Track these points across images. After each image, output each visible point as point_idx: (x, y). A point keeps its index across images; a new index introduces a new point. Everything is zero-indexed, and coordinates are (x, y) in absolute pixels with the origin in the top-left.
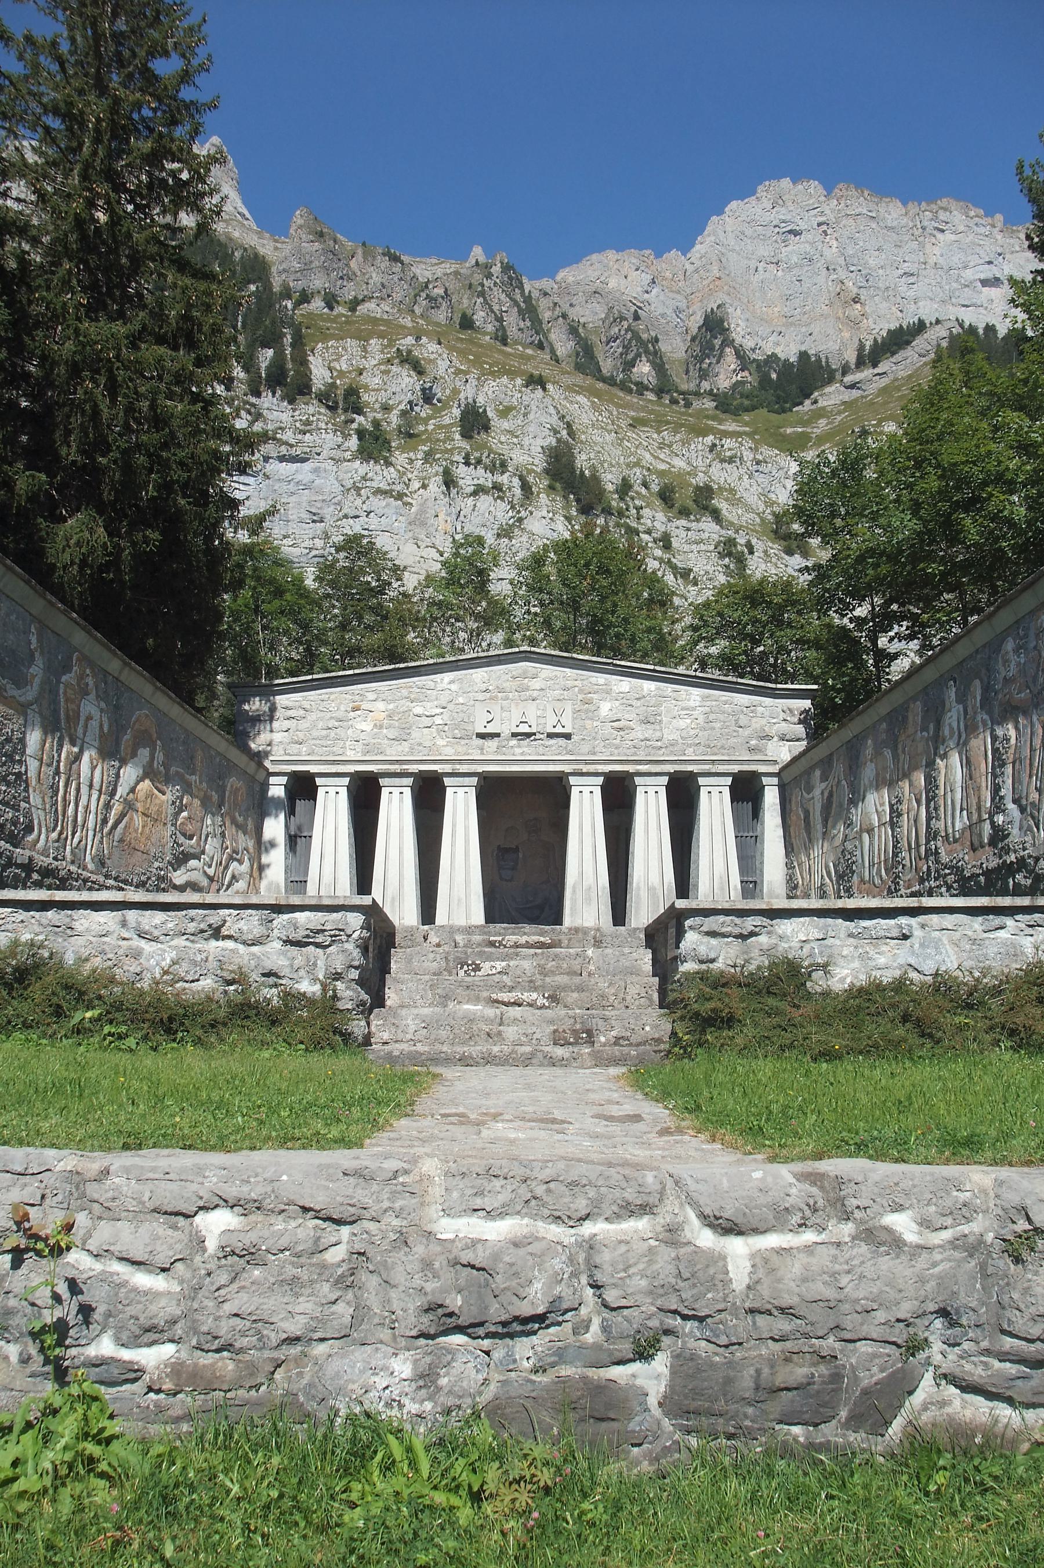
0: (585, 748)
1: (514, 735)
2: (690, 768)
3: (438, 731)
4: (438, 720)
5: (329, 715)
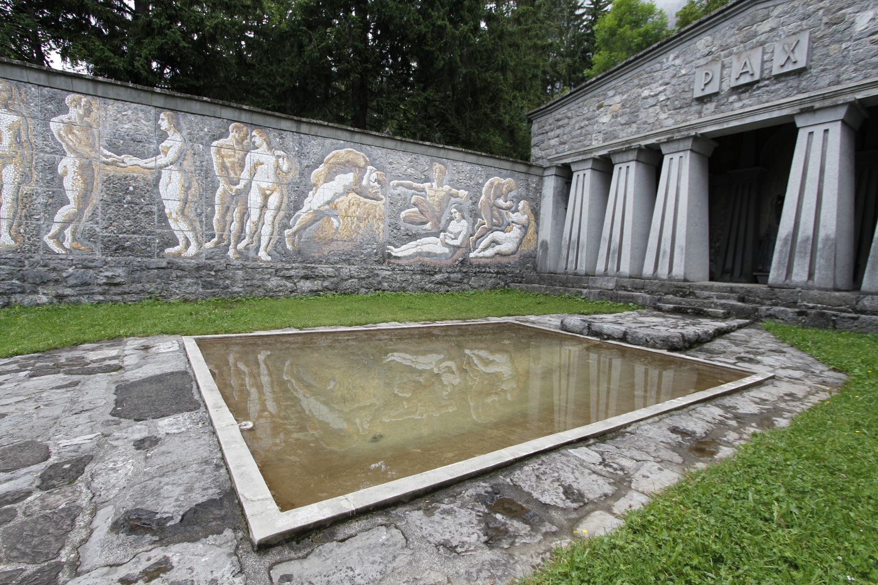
1: (735, 90)
3: (662, 107)
4: (662, 98)
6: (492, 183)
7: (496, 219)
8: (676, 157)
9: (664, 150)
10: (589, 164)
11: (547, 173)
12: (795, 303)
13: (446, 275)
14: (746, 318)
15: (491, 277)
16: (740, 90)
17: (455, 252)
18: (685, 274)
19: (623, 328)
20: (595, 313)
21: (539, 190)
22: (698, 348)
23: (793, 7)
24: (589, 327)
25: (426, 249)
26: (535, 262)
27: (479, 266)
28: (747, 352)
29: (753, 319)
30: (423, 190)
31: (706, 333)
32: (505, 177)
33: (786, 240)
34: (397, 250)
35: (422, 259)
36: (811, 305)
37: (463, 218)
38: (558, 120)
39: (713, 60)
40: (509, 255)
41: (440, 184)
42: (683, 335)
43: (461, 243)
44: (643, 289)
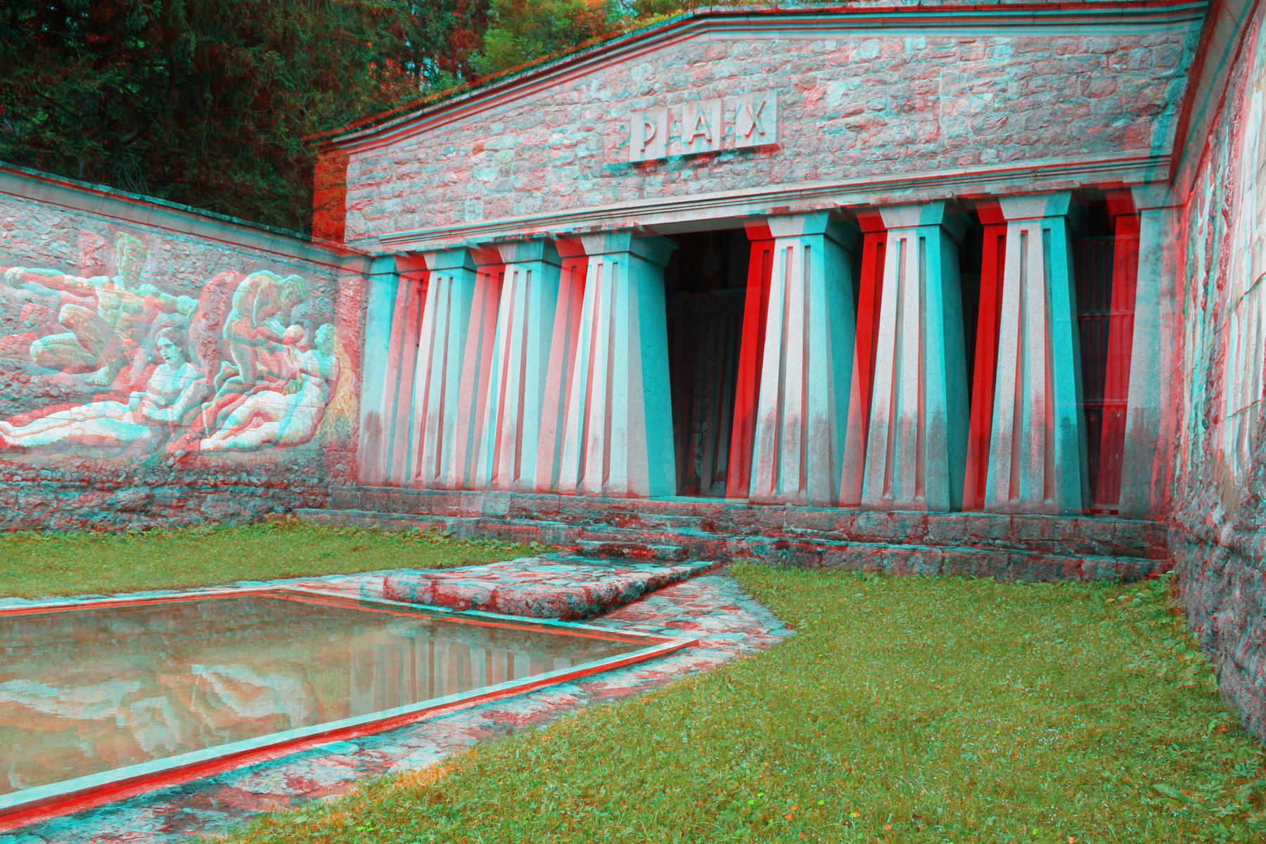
0: (802, 169)
1: (688, 158)
2: (991, 188)
3: (582, 169)
5: (445, 164)
6: (255, 285)
7: (264, 362)
8: (607, 262)
9: (589, 245)
10: (460, 259)
11: (376, 268)
12: (780, 528)
13: (144, 491)
14: (709, 559)
15: (252, 495)
16: (696, 162)
17: (166, 438)
18: (630, 482)
19: (491, 586)
20: (464, 564)
21: (361, 304)
22: (617, 612)
23: (755, 49)
24: (434, 589)
25: (92, 429)
26: (354, 461)
27: (223, 469)
28: (688, 613)
29: (716, 559)
30: (89, 292)
31: (630, 585)
32: (284, 272)
33: (769, 420)
34: (19, 431)
35: (83, 453)
36: (799, 531)
37: (187, 358)
38: (400, 163)
39: (656, 104)
40: (294, 445)
41: (133, 280)
42: (588, 591)
43: (181, 417)
44: (558, 513)
